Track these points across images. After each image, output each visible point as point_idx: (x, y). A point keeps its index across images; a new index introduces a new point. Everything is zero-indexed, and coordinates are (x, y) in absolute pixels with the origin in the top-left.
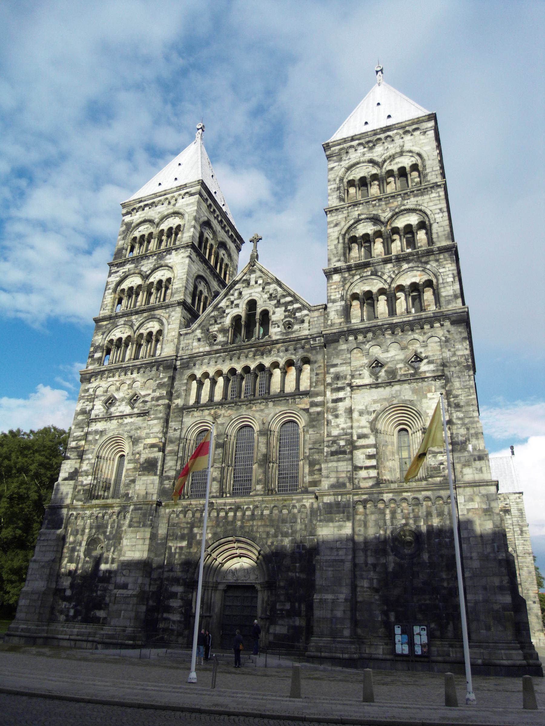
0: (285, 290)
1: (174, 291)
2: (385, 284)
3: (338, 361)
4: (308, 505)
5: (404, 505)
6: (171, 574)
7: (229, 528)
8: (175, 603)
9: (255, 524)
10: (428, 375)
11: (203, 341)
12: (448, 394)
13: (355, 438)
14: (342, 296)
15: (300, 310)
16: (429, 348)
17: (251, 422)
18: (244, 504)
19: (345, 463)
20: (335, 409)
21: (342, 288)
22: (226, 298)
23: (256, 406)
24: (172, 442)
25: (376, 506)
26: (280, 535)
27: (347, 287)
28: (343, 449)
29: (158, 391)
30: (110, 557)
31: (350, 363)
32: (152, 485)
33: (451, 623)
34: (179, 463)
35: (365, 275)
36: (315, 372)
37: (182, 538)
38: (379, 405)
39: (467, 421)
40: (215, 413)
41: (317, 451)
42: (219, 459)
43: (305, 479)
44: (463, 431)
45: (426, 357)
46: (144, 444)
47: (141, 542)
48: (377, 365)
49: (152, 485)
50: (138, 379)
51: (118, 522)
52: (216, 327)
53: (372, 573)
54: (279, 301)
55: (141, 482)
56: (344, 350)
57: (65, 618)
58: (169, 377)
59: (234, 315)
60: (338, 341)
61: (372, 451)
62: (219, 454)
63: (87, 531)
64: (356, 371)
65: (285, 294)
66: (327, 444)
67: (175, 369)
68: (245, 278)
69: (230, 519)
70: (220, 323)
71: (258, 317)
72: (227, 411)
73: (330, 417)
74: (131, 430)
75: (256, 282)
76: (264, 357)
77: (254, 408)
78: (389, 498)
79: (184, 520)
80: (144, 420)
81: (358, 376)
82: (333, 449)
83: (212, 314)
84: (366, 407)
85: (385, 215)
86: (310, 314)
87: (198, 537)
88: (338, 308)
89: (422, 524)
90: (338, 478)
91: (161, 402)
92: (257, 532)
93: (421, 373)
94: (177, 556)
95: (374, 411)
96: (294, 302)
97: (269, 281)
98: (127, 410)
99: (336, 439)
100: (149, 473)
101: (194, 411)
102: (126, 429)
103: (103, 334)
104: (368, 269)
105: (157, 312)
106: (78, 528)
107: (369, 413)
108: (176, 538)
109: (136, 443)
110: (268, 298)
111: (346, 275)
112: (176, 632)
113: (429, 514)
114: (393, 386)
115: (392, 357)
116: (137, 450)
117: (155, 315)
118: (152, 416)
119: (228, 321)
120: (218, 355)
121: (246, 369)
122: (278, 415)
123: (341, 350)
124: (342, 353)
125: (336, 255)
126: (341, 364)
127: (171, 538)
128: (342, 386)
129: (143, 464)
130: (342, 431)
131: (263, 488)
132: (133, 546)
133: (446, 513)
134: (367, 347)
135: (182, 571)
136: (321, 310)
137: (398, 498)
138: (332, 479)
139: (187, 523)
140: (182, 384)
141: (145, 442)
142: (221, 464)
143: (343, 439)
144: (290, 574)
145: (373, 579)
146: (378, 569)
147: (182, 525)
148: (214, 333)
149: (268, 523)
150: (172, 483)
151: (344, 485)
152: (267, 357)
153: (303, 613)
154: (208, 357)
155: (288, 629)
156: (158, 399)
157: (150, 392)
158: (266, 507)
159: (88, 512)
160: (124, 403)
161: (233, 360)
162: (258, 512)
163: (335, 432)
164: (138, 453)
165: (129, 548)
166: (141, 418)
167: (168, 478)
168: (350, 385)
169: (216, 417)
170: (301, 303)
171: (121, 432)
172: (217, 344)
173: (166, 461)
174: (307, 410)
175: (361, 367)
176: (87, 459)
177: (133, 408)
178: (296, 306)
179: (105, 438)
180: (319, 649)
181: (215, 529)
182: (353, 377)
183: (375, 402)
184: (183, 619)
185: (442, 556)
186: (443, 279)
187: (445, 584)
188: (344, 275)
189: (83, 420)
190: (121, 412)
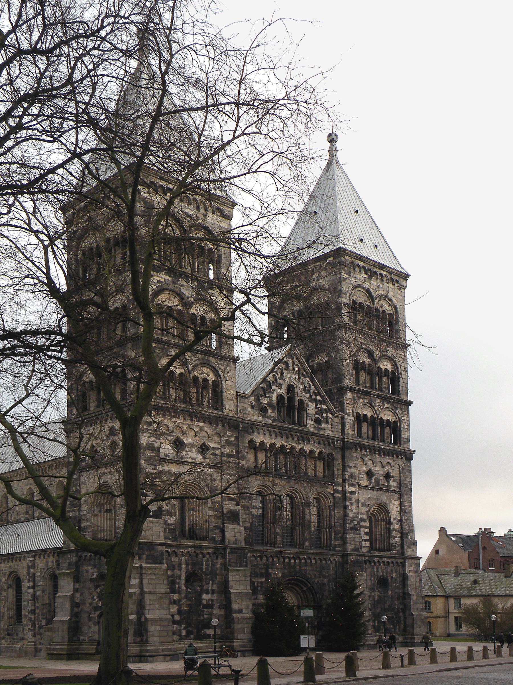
3: (353, 465)
4: (337, 559)
5: (382, 565)
6: (257, 601)
7: (292, 570)
10: (393, 489)
11: (257, 410)
12: (401, 504)
15: (326, 411)
16: (395, 472)
20: (351, 499)
22: (272, 374)
25: (370, 564)
37: (261, 576)
39: (408, 521)
40: (273, 480)
44: (407, 527)
45: (393, 477)
48: (370, 474)
50: (206, 429)
51: (212, 561)
52: (265, 401)
54: (311, 396)
57: (178, 637)
60: (351, 449)
61: (367, 530)
63: (184, 566)
64: (360, 474)
69: (292, 564)
70: (268, 397)
71: (297, 404)
73: (348, 503)
75: (294, 369)
79: (261, 563)
82: (351, 526)
83: (262, 385)
85: (377, 354)
90: (355, 545)
91: (231, 459)
94: (259, 588)
98: (199, 458)
105: (212, 359)
106: (174, 564)
113: (392, 571)
117: (209, 361)
119: (274, 397)
120: (273, 429)
124: (354, 458)
134: (367, 459)
137: (381, 561)
139: (264, 565)
154: (265, 429)
156: (229, 456)
157: (218, 446)
159: (184, 551)
162: (308, 561)
164: (217, 503)
168: (357, 483)
169: (274, 485)
172: (268, 417)
174: (333, 495)
177: (204, 458)
178: (324, 407)
185: (396, 593)
189: (153, 457)
190: (192, 458)
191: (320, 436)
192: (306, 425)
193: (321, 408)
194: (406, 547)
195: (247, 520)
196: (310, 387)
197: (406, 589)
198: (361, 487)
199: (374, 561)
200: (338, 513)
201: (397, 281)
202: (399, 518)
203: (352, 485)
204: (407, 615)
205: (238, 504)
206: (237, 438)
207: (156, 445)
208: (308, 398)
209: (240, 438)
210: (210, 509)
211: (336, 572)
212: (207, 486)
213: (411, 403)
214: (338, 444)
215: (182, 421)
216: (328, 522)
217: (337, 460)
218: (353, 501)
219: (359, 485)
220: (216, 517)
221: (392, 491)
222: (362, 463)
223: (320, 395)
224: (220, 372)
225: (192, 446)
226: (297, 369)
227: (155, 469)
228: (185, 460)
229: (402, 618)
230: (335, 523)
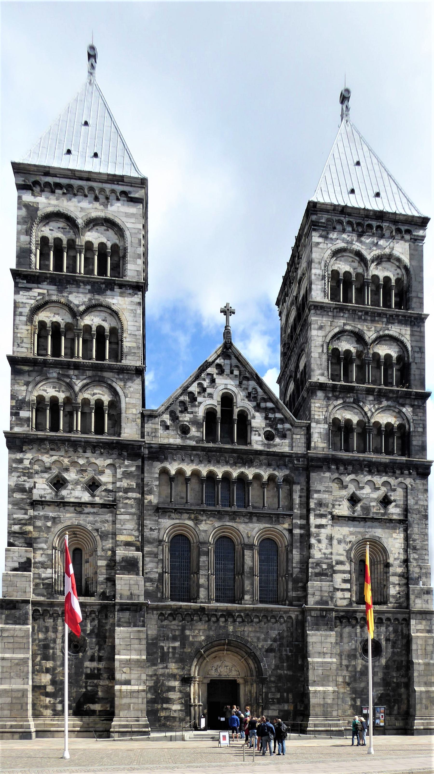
0: (265, 392)
1: (125, 350)
3: (322, 488)
4: (293, 616)
6: (167, 671)
7: (221, 632)
8: (173, 695)
9: (245, 629)
10: (395, 517)
13: (334, 563)
14: (326, 418)
15: (282, 421)
17: (231, 534)
20: (318, 535)
21: (326, 409)
22: (197, 382)
23: (239, 518)
24: (150, 543)
26: (269, 640)
27: (331, 408)
29: (124, 480)
30: (96, 655)
31: (331, 492)
33: (397, 705)
34: (160, 565)
35: (348, 400)
37: (174, 639)
38: (354, 537)
42: (204, 566)
44: (417, 570)
46: (116, 541)
47: (137, 641)
53: (345, 672)
55: (123, 582)
56: (327, 477)
58: (137, 467)
59: (208, 407)
60: (321, 467)
61: (347, 576)
62: (204, 561)
64: (336, 501)
65: (266, 397)
68: (218, 361)
70: (192, 413)
71: (235, 417)
72: (209, 518)
74: (96, 521)
75: (232, 372)
77: (238, 520)
78: (360, 617)
83: (182, 398)
84: (344, 536)
86: (293, 429)
87: (191, 639)
88: (322, 430)
89: (382, 637)
91: (130, 495)
92: (248, 636)
93: (389, 514)
94: (171, 655)
95: (350, 542)
96: (276, 410)
97: (247, 375)
98: (86, 497)
102: (88, 519)
104: (351, 394)
105: (107, 375)
107: (346, 543)
108: (166, 638)
109: (105, 538)
110: (247, 397)
112: (177, 719)
114: (366, 522)
115: (367, 494)
117: (104, 377)
119: (201, 412)
120: (194, 452)
121: (227, 476)
124: (324, 480)
125: (320, 367)
127: (161, 639)
128: (324, 513)
130: (323, 556)
131: (251, 598)
132: (128, 645)
133: (400, 631)
135: (177, 669)
136: (303, 428)
139: (178, 626)
140: (154, 477)
141: (117, 539)
144: (279, 671)
145: (346, 676)
146: (350, 669)
147: (172, 627)
148: (185, 423)
149: (258, 629)
150: (155, 585)
151: (326, 603)
152: (249, 467)
153: (291, 701)
154: (183, 452)
155: (279, 713)
156: (126, 491)
160: (79, 487)
161: (212, 462)
165: (122, 647)
166: (106, 510)
168: (331, 513)
170: (283, 414)
171: (81, 522)
172: (190, 438)
173: (145, 563)
175: (341, 498)
176: (40, 549)
177: (93, 496)
178: (278, 415)
179: (60, 527)
180: (315, 725)
181: (207, 632)
183: (351, 533)
184: (183, 708)
187: (395, 680)
188: (328, 395)
189: (23, 499)
190: (77, 498)
191: (268, 454)
192: (250, 443)
193: (275, 418)
194: (412, 597)
195: (155, 570)
196: (257, 392)
197: (410, 656)
198: (336, 519)
199: (356, 619)
200: (296, 555)
201: (408, 232)
202: (402, 557)
203: (322, 516)
204: (410, 691)
205: (137, 550)
206: (141, 469)
207: (27, 486)
208: (254, 407)
209: (146, 468)
210: (102, 558)
211: (292, 634)
212: (97, 530)
213: (428, 395)
214: (301, 463)
215: (63, 453)
216: (285, 568)
217: (298, 484)
218: (323, 537)
221: (391, 520)
223: (273, 402)
224: (118, 389)
225: (77, 483)
226: (236, 372)
227: (26, 514)
228: (66, 500)
229: (404, 697)
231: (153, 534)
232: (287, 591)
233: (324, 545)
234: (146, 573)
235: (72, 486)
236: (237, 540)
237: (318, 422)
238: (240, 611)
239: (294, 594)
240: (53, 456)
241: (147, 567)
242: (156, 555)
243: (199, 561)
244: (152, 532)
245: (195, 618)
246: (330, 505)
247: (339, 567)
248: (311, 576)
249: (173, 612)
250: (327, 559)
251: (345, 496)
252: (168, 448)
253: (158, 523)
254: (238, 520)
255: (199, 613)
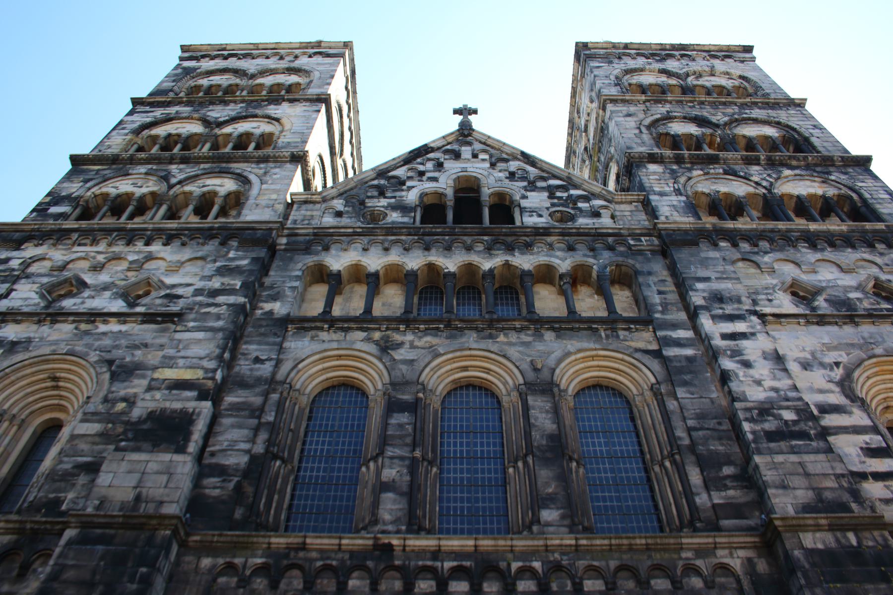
2: (759, 187)
4: (736, 564)
17: (488, 371)
18: (510, 556)
19: (821, 457)
23: (506, 335)
28: (797, 428)
32: (165, 478)
34: (263, 436)
36: (654, 288)
40: (386, 339)
41: (715, 434)
42: (401, 437)
43: (698, 500)
49: (165, 478)
58: (254, 260)
62: (401, 426)
66: (748, 415)
67: (273, 250)
68: (449, 147)
72: (420, 338)
74: (117, 347)
76: (516, 254)
80: (164, 330)
81: (767, 303)
84: (813, 354)
91: (221, 299)
99: (766, 406)
100: (154, 446)
101: (322, 329)
102: (97, 344)
103: (86, 181)
111: (675, 167)
116: (122, 393)
118: (192, 324)
122: (573, 358)
123: (707, 258)
126: (717, 278)
128: (736, 312)
129: (140, 421)
131: (563, 517)
138: (800, 493)
140: (290, 276)
142: (408, 449)
143: (787, 408)
150: (231, 485)
152: (522, 254)
158: (590, 568)
160: (107, 294)
163: (757, 395)
167: (222, 471)
173: (217, 429)
182: (755, 302)
183: (830, 348)
186: (871, 195)
193: (570, 196)
219: (762, 316)
220: (104, 437)
222: (753, 271)
224: (252, 178)
230: (689, 430)
231: (258, 369)
232: (689, 493)
233: (763, 370)
234: (213, 454)
235: (93, 293)
236: (505, 383)
237: (662, 194)
238: (527, 555)
239: (718, 498)
240: (78, 252)
241: (220, 438)
242: (257, 412)
243: (386, 424)
244: (257, 366)
245: (352, 583)
246: (744, 299)
247: (831, 420)
248: (755, 441)
249: (271, 561)
250: (787, 400)
251: (776, 285)
252: (332, 235)
253: (281, 349)
254: (502, 338)
255: (370, 564)
